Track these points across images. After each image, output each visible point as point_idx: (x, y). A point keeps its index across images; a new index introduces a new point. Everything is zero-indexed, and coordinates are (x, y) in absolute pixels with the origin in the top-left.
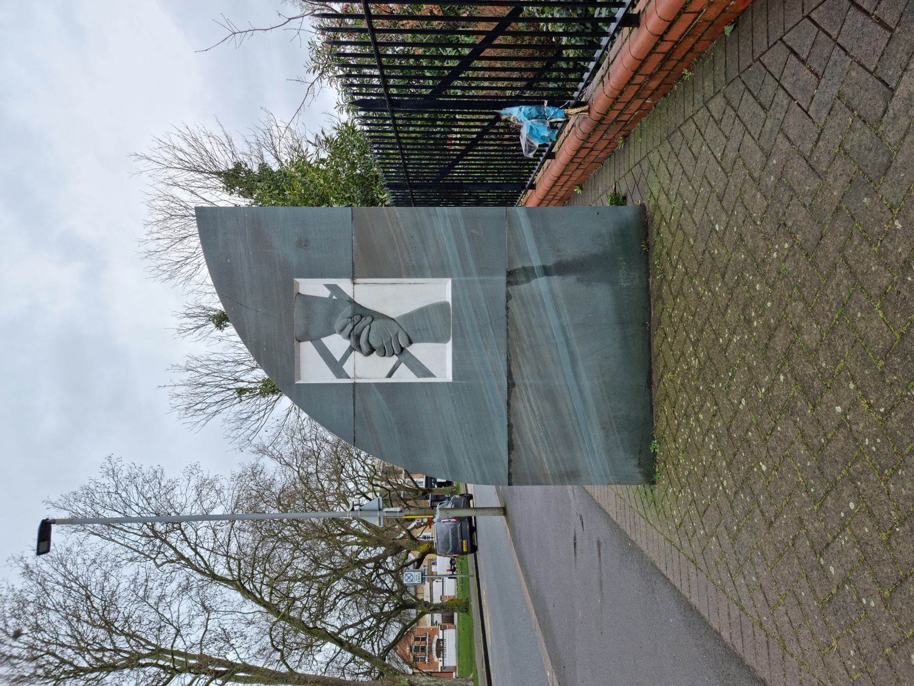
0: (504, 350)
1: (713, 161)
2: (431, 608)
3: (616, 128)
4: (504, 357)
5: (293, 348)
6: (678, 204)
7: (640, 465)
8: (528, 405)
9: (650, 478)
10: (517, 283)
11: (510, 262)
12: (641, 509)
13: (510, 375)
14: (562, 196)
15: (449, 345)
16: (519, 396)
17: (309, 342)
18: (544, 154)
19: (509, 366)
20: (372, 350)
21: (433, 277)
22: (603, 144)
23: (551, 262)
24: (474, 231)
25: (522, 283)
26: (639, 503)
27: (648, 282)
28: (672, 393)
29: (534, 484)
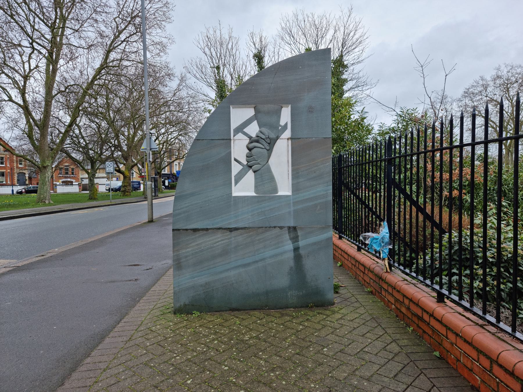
0: (251, 225)
1: (362, 346)
2: (92, 177)
3: (376, 287)
4: (247, 226)
5: (251, 104)
6: (337, 325)
7: (185, 305)
9: (177, 311)
10: (289, 232)
11: (301, 229)
12: (159, 305)
13: (236, 229)
14: (340, 257)
15: (254, 194)
16: (225, 234)
18: (360, 245)
19: (242, 229)
20: (250, 149)
21: (292, 184)
22: (368, 280)
23: (302, 252)
24: (319, 208)
25: (290, 236)
26: (162, 305)
27: (291, 308)
28: (227, 324)
29: (173, 244)
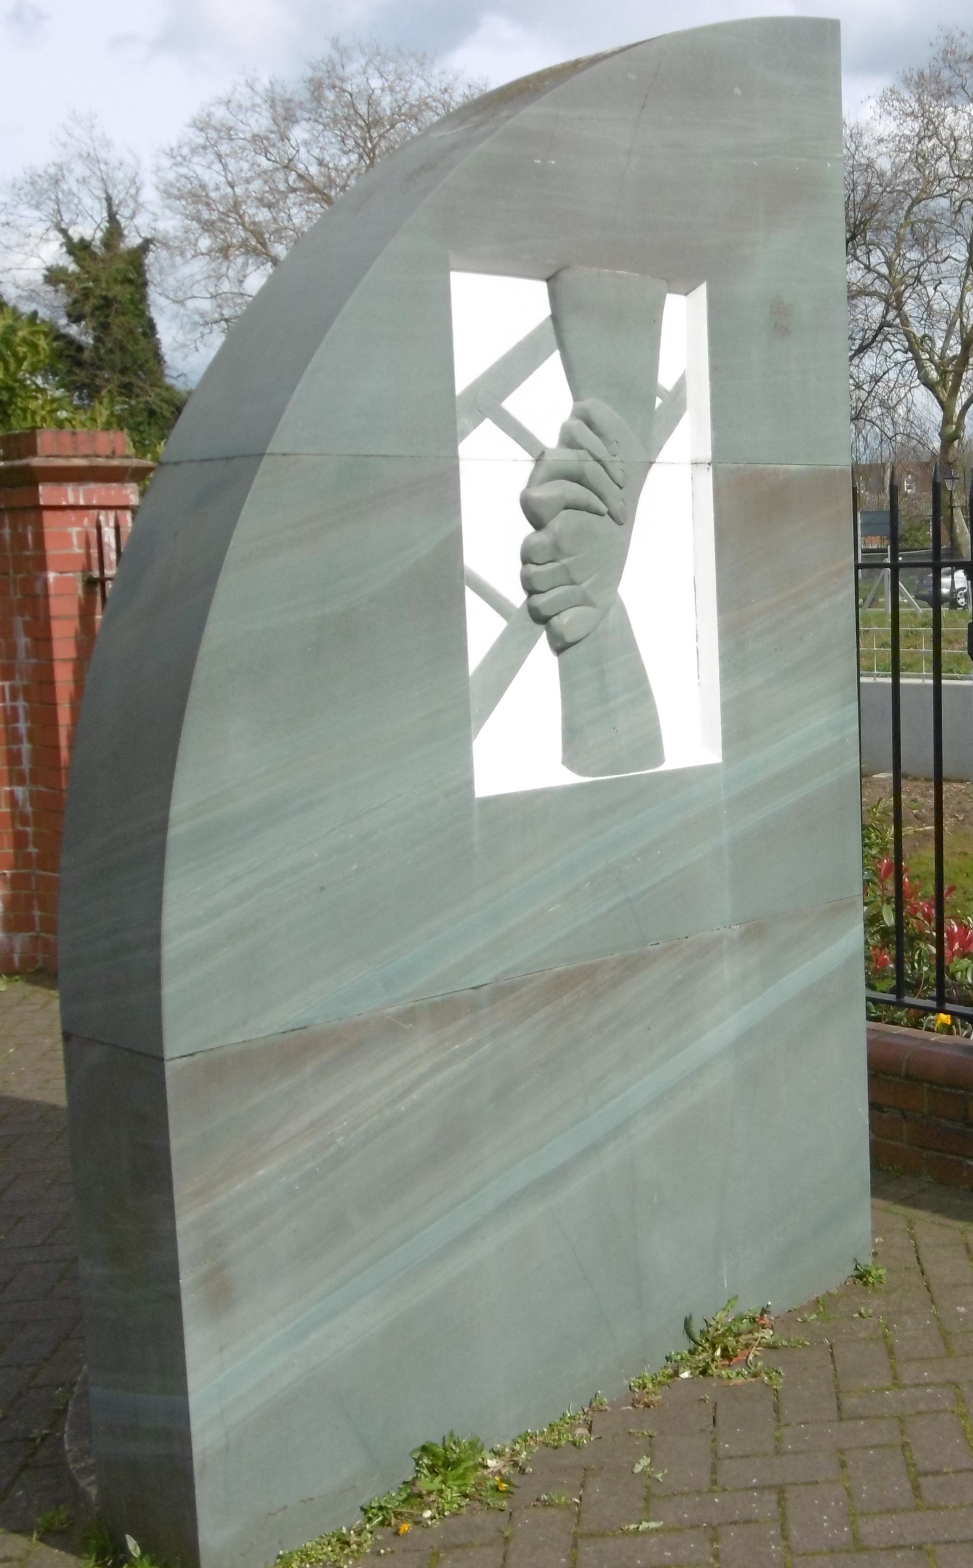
8: (424, 1068)
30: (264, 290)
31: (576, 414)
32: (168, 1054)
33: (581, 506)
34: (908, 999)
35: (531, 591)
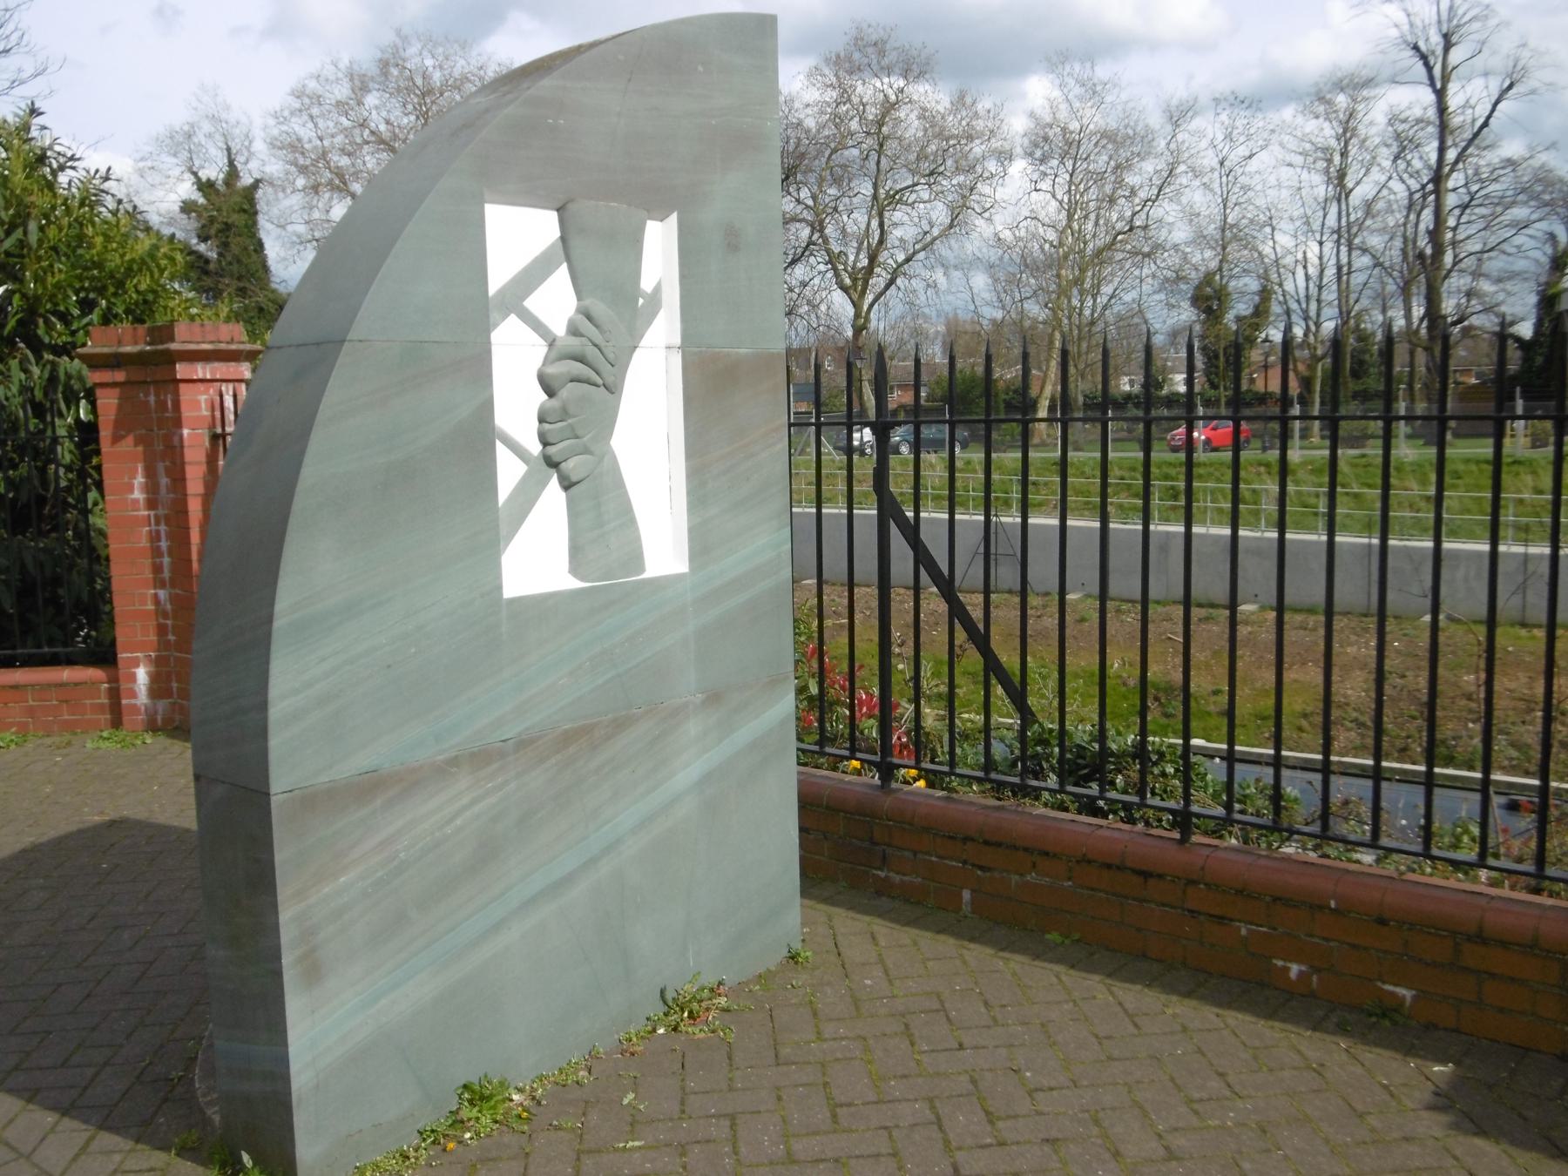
8: (465, 800)
17: (558, 234)
30: (345, 218)
31: (579, 310)
32: (273, 791)
33: (583, 380)
34: (828, 750)
35: (545, 443)
